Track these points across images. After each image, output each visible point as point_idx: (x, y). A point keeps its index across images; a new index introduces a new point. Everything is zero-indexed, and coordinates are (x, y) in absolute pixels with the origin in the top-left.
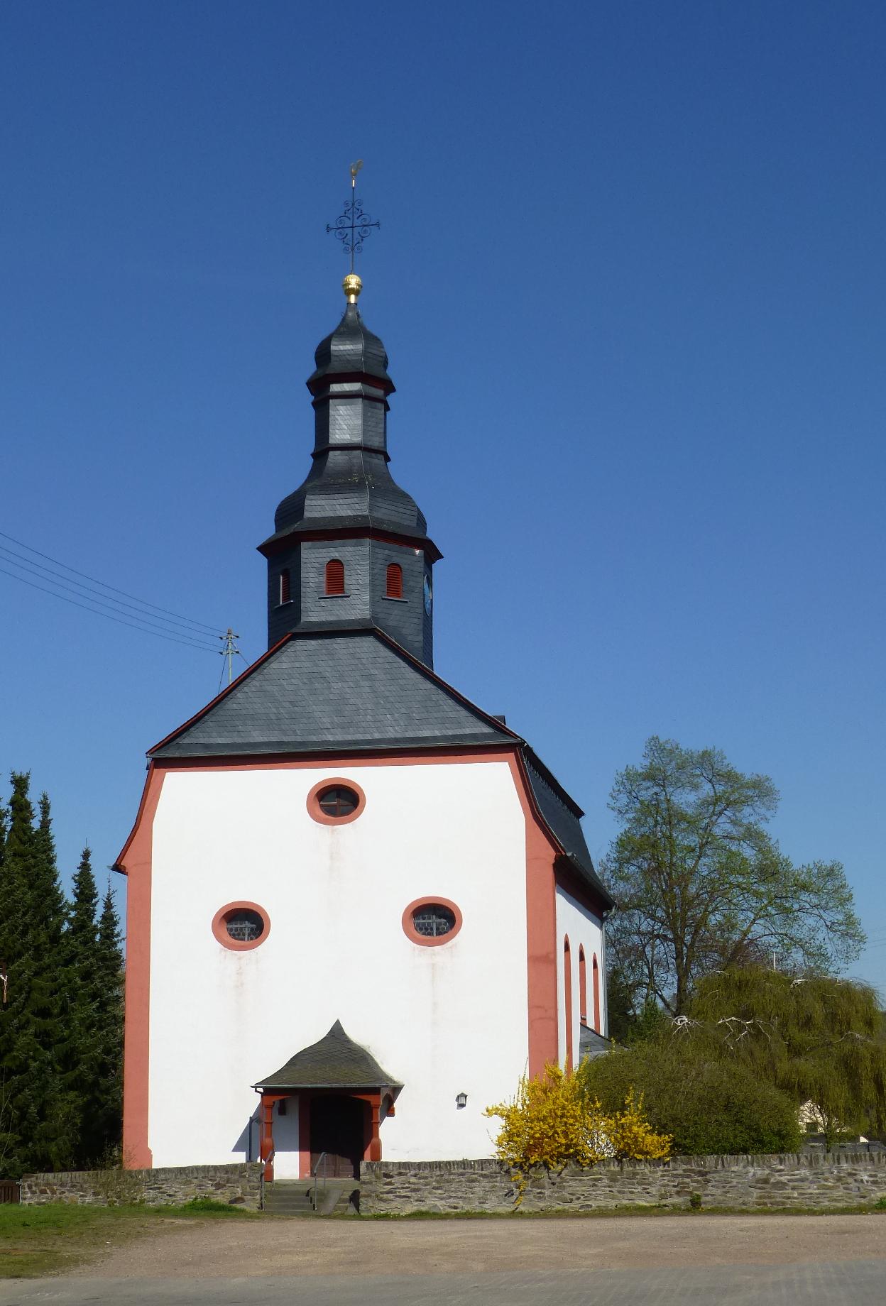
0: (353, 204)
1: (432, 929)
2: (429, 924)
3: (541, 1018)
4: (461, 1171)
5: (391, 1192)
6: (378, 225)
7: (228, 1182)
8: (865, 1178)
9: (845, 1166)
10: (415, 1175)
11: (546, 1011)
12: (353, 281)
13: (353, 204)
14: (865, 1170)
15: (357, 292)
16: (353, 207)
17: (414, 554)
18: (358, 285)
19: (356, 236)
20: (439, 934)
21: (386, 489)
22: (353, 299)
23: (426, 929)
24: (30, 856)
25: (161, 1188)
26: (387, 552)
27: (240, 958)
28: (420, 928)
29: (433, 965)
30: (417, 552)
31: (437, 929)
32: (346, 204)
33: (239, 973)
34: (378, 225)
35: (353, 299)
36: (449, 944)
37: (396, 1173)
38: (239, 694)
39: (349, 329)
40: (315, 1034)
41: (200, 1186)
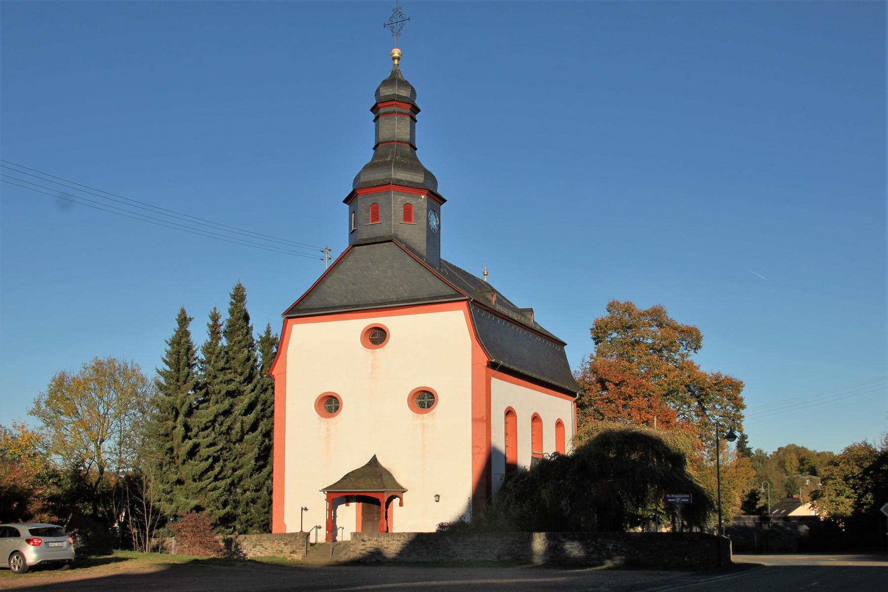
0: (397, 10)
1: (425, 405)
2: (423, 402)
3: (479, 453)
4: (399, 538)
5: (365, 550)
6: (409, 19)
7: (290, 542)
8: (610, 547)
9: (599, 540)
10: (376, 540)
11: (481, 449)
12: (396, 53)
13: (397, 10)
14: (611, 543)
15: (399, 59)
16: (397, 11)
17: (421, 198)
18: (399, 54)
19: (399, 27)
20: (338, 403)
21: (416, 166)
22: (396, 62)
23: (422, 405)
24: (233, 370)
25: (262, 545)
26: (403, 197)
27: (328, 422)
28: (429, 407)
29: (423, 424)
30: (423, 197)
31: (428, 404)
32: (393, 10)
33: (328, 430)
34: (409, 19)
35: (396, 62)
36: (432, 412)
37: (367, 539)
38: (328, 282)
39: (394, 79)
40: (361, 462)
41: (278, 544)
